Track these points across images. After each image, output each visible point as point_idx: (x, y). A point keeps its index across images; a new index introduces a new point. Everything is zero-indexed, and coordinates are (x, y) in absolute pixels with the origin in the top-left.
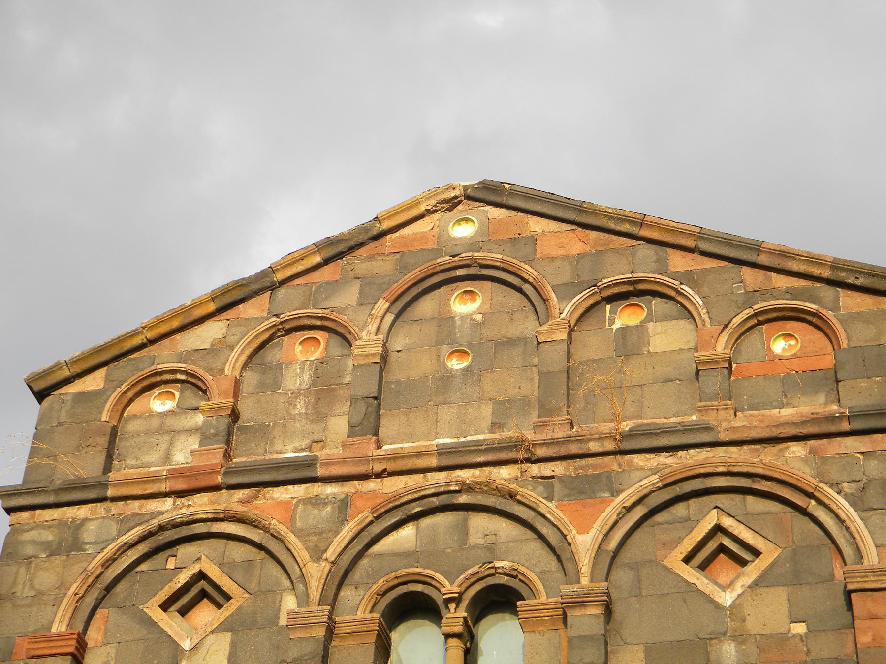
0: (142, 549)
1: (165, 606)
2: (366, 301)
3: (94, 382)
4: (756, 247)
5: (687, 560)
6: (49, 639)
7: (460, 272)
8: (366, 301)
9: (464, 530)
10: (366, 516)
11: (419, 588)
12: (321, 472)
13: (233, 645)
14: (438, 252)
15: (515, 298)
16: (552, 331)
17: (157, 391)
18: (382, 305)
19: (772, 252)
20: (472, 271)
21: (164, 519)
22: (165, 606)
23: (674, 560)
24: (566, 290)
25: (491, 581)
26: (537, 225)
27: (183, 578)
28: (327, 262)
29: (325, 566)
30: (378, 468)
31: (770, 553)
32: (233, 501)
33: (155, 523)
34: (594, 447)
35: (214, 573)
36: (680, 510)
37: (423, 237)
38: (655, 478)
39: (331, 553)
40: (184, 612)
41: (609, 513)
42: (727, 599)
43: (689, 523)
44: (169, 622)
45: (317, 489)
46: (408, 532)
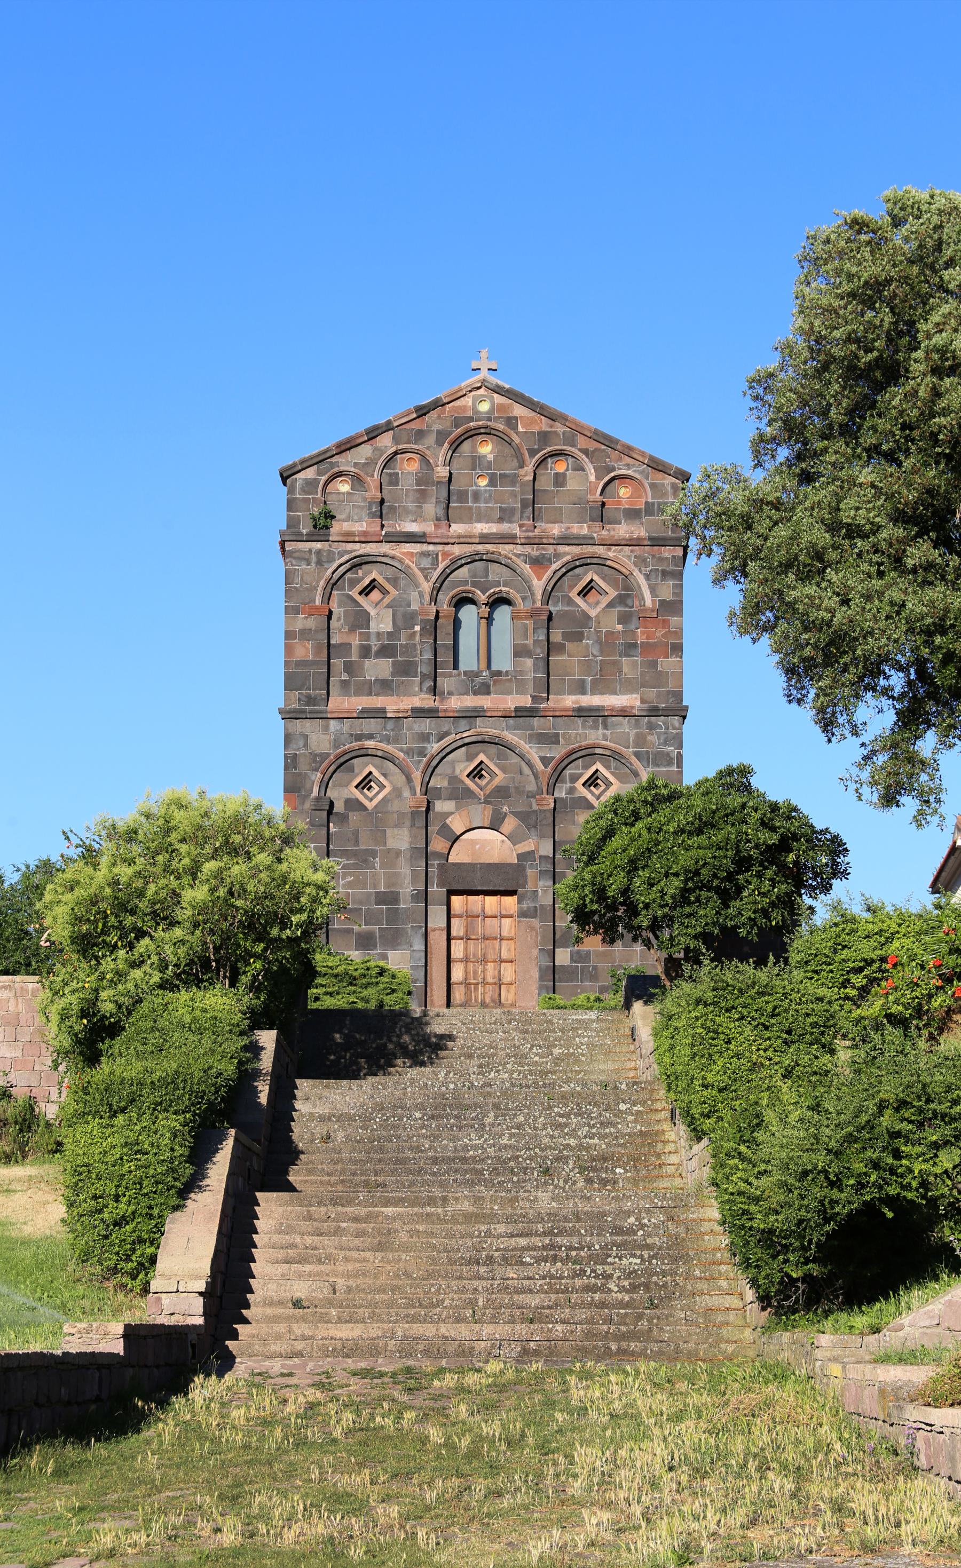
0: (348, 566)
1: (360, 593)
2: (440, 443)
3: (310, 473)
4: (617, 441)
5: (579, 594)
6: (317, 608)
7: (482, 431)
8: (440, 443)
9: (486, 571)
10: (447, 562)
11: (470, 595)
12: (429, 540)
13: (394, 615)
14: (471, 419)
15: (508, 450)
16: (525, 475)
17: (340, 479)
18: (446, 445)
19: (623, 446)
20: (488, 431)
21: (357, 553)
22: (360, 593)
23: (573, 594)
24: (532, 453)
25: (499, 595)
26: (519, 411)
27: (367, 581)
28: (418, 417)
29: (431, 584)
30: (453, 541)
31: (613, 593)
32: (385, 548)
33: (353, 554)
34: (545, 541)
35: (380, 579)
36: (577, 571)
37: (464, 408)
38: (568, 558)
39: (434, 579)
40: (367, 595)
41: (549, 573)
42: (593, 613)
43: (579, 578)
44: (361, 599)
45: (425, 547)
46: (465, 569)
